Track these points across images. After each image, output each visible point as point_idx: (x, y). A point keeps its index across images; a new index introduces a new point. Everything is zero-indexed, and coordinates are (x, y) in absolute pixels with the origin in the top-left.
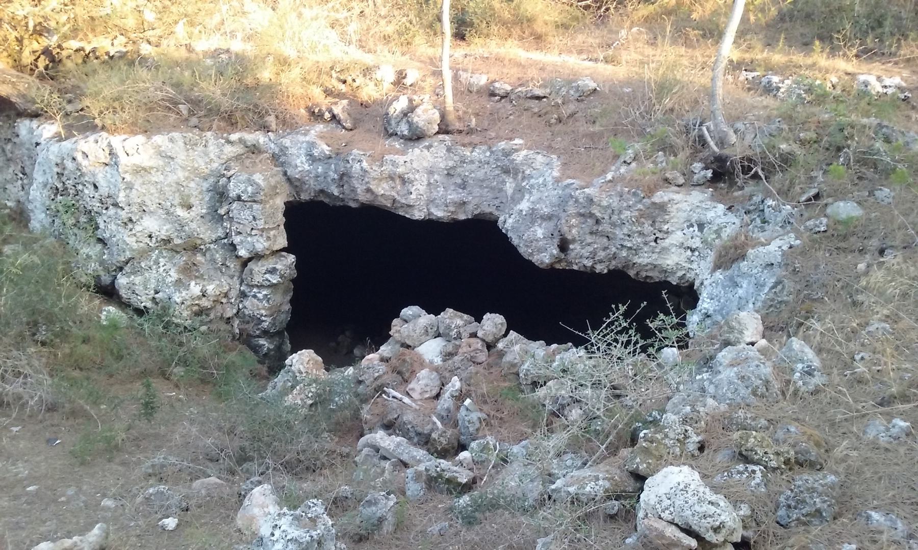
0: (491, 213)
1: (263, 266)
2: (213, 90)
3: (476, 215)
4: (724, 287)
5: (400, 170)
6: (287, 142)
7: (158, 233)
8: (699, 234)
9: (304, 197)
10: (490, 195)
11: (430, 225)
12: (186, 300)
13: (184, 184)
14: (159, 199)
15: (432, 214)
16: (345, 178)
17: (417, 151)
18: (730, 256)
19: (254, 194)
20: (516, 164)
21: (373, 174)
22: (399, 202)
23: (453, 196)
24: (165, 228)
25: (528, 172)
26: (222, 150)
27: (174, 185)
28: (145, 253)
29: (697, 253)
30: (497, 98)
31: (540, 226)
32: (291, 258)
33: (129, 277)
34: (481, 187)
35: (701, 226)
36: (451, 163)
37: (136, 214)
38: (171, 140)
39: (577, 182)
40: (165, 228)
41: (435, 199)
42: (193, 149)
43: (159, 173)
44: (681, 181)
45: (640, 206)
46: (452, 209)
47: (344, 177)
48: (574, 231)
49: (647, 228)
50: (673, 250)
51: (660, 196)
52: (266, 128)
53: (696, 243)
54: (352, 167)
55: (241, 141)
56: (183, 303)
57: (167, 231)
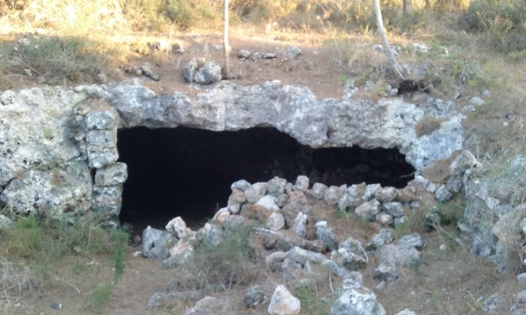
0: (266, 123)
1: (111, 172)
2: (63, 59)
3: (257, 125)
4: (431, 143)
5: (209, 102)
6: (120, 89)
7: (31, 159)
8: (402, 120)
9: (132, 124)
10: (264, 113)
11: (227, 134)
12: (63, 201)
13: (46, 122)
14: (30, 134)
15: (228, 127)
16: (170, 109)
17: (215, 90)
18: (426, 129)
19: (107, 124)
20: (285, 93)
21: (194, 105)
22: (208, 121)
23: (242, 115)
24: (36, 154)
25: (293, 97)
26: (72, 98)
27: (40, 124)
28: (21, 175)
29: (402, 130)
30: (244, 59)
31: (314, 125)
32: (124, 166)
33: (15, 191)
34: (259, 108)
35: (402, 116)
36: (237, 96)
37: (13, 146)
38: (34, 93)
39: (334, 100)
40: (36, 154)
41: (231, 118)
42: (50, 98)
43: (27, 116)
44: (386, 95)
45: (373, 109)
46: (242, 122)
47: (170, 109)
48: (337, 125)
49: (377, 119)
50: (389, 130)
51: (382, 102)
52: (98, 82)
53: (401, 125)
54: (177, 102)
55: (84, 90)
56: (60, 204)
57: (38, 156)
